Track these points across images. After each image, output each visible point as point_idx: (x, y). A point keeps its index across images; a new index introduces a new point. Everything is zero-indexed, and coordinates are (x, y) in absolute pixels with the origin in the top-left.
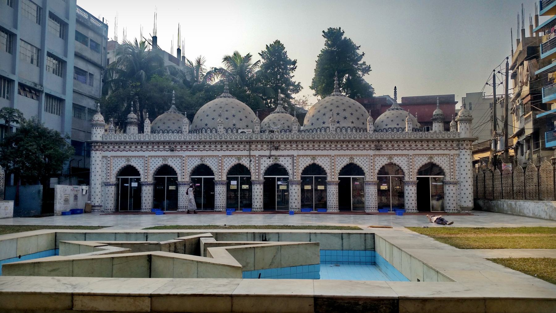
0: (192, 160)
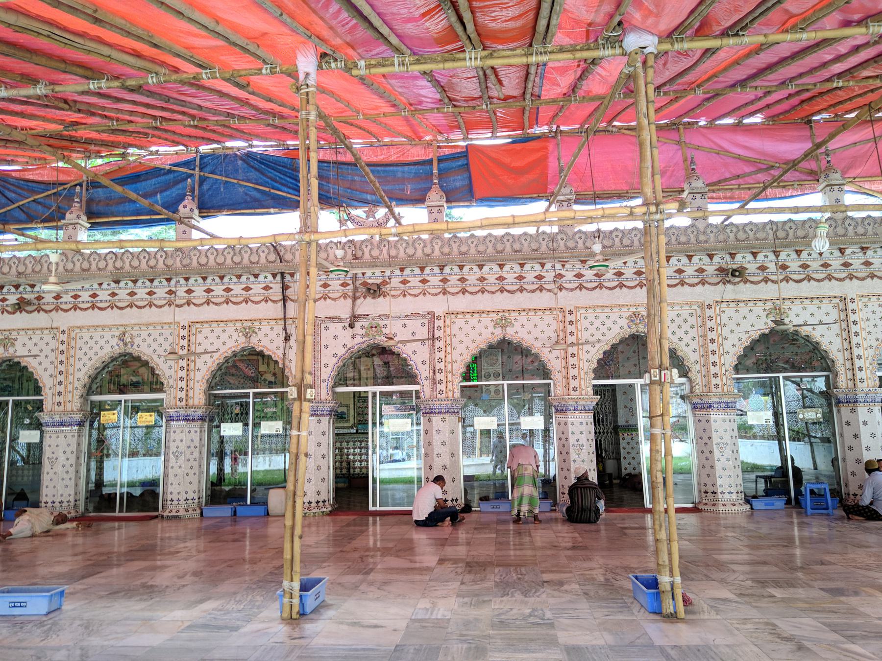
0: (91, 343)
